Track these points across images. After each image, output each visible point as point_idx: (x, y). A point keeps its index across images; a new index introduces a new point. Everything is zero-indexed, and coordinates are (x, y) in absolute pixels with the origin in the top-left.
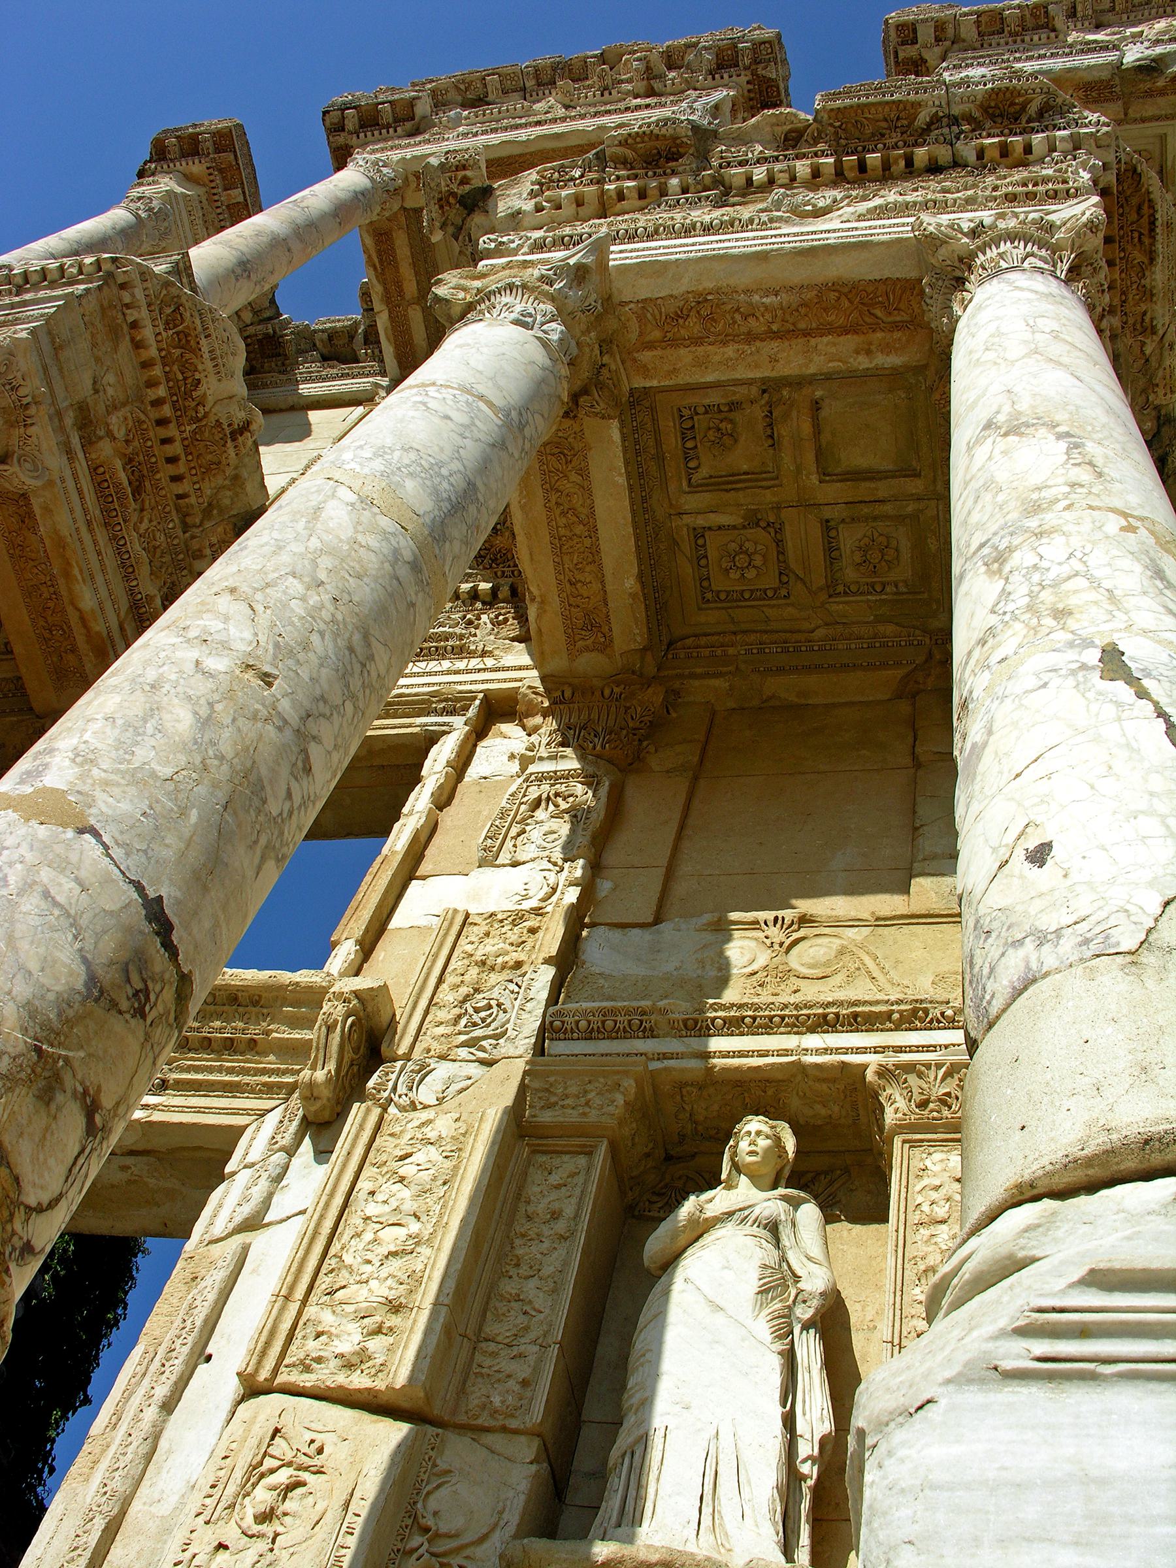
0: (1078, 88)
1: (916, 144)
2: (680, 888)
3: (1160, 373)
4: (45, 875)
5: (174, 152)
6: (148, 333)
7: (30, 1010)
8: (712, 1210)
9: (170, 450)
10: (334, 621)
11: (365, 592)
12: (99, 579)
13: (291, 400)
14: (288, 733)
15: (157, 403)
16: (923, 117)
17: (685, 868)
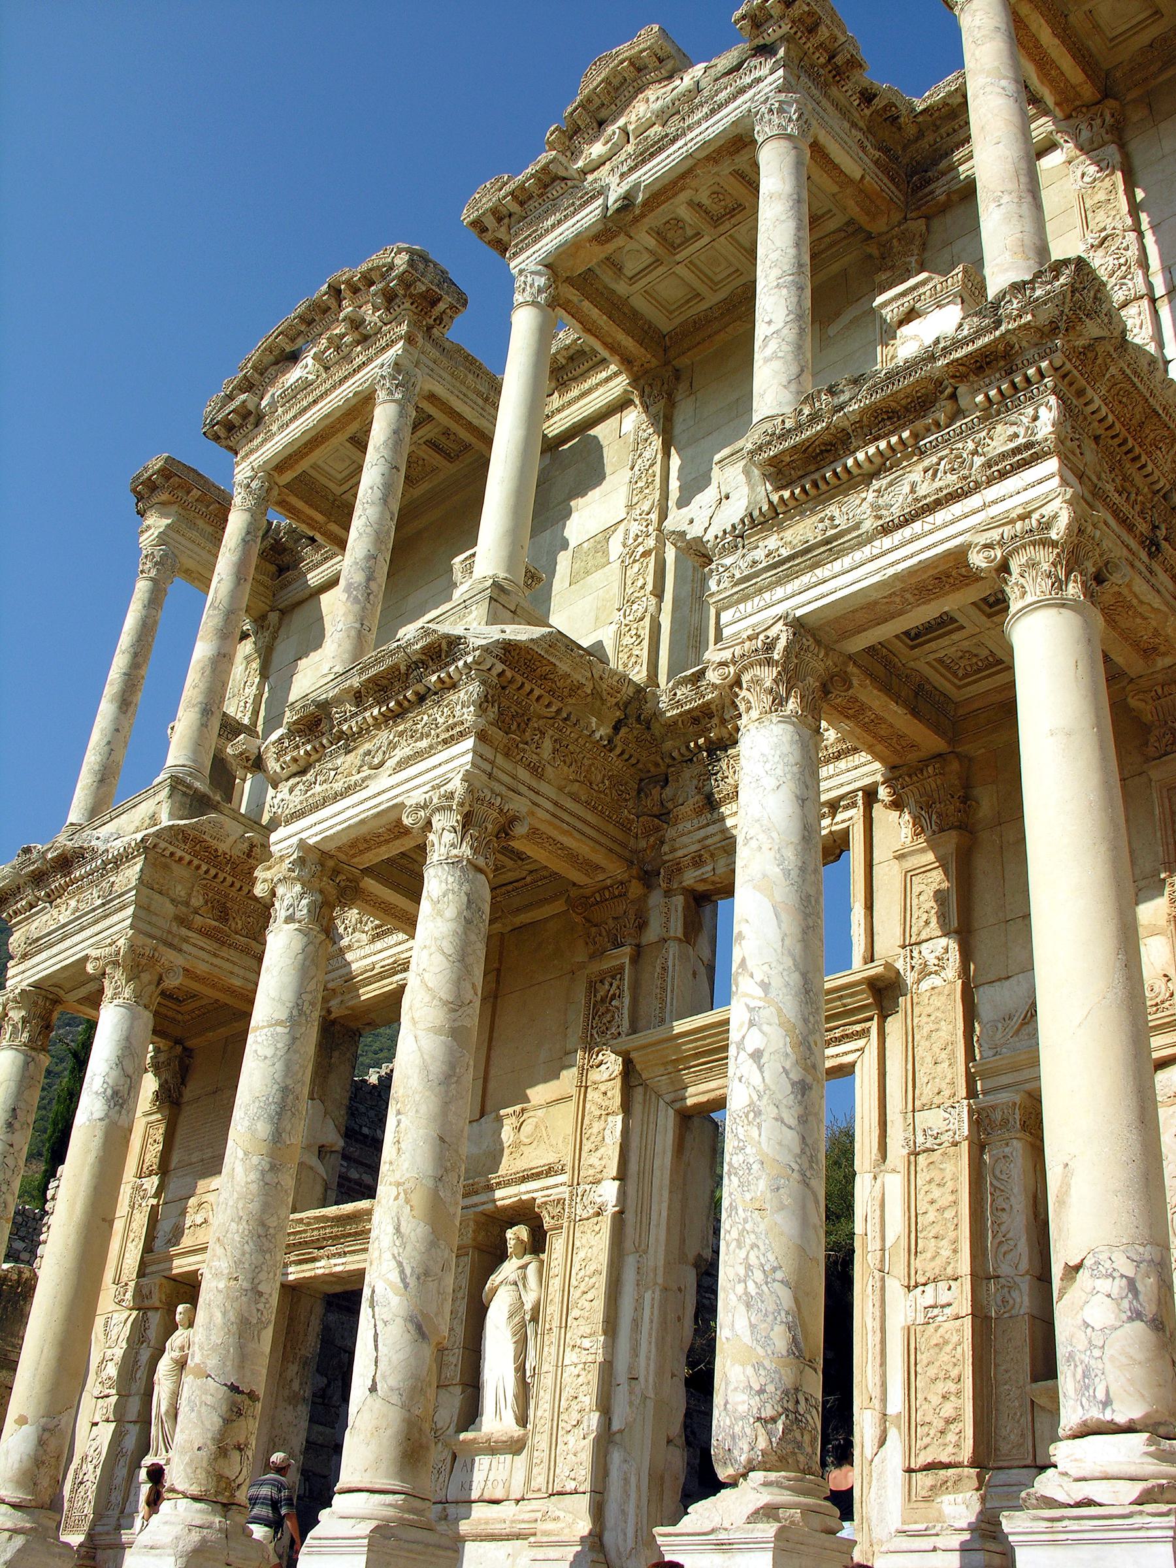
0: (590, 241)
1: (407, 688)
2: (492, 1085)
3: (604, 693)
4: (203, 1398)
5: (146, 494)
6: (179, 853)
7: (213, 1439)
8: (496, 1283)
9: (227, 884)
10: (250, 1231)
11: (255, 1207)
12: (236, 969)
13: (307, 592)
14: (249, 1293)
15: (207, 872)
16: (403, 668)
17: (492, 1072)
